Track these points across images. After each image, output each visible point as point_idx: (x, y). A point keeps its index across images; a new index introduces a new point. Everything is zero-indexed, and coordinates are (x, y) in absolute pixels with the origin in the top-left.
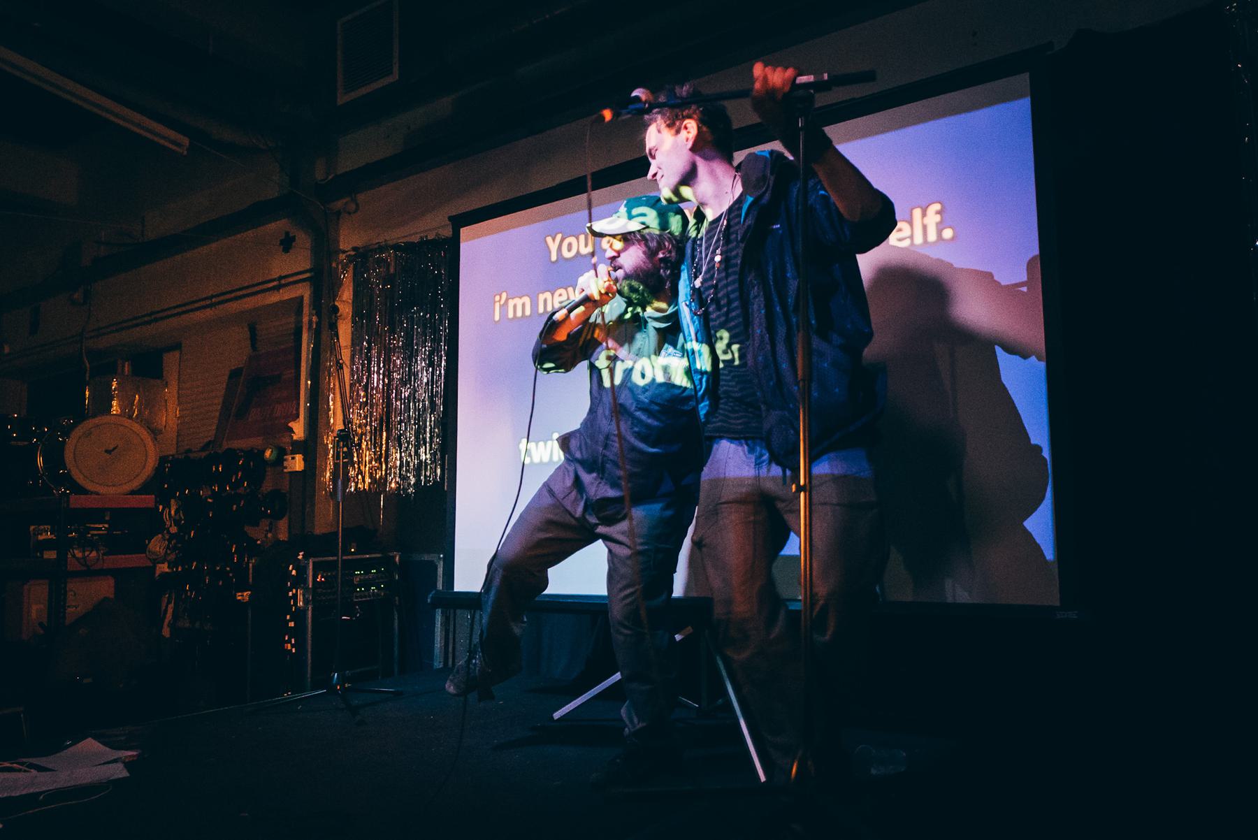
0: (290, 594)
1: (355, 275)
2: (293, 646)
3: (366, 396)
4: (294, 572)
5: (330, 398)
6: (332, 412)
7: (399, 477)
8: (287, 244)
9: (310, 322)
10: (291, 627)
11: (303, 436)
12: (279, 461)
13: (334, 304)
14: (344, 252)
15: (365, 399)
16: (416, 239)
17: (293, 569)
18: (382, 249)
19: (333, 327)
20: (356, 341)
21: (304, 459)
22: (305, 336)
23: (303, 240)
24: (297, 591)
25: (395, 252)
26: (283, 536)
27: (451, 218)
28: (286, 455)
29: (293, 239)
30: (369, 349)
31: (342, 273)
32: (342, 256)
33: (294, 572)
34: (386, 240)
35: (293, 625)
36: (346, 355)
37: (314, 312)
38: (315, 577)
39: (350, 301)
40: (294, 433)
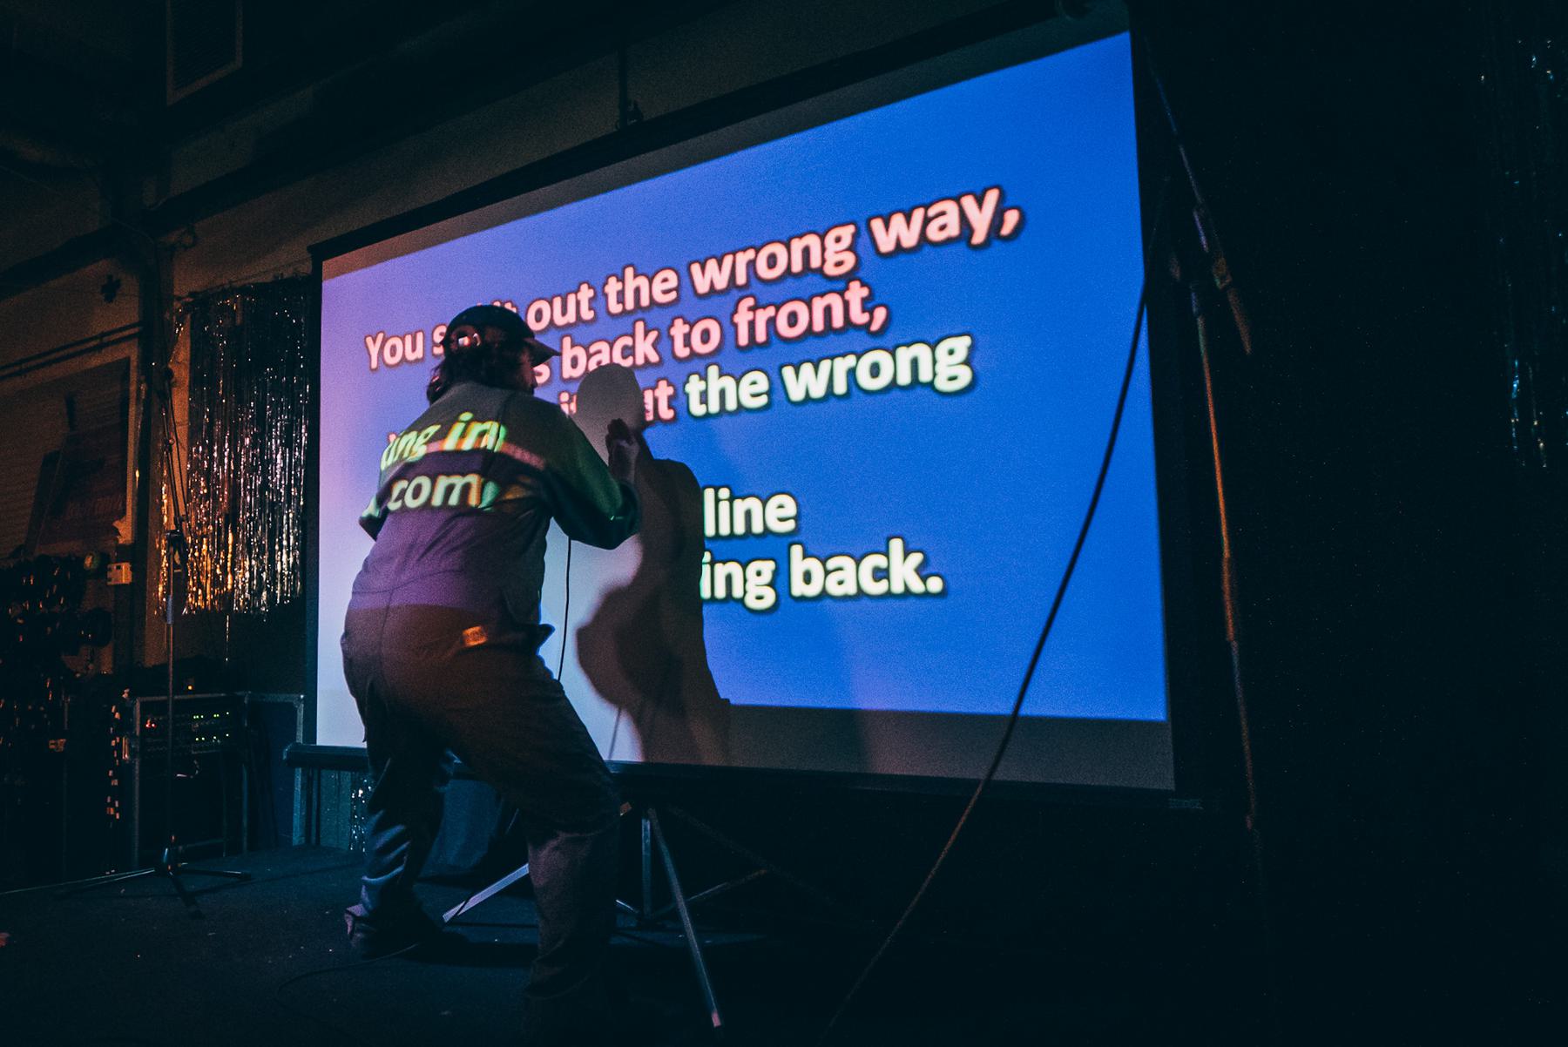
0: (113, 743)
1: (192, 328)
2: (117, 810)
3: (207, 487)
4: (117, 715)
5: (163, 489)
6: (165, 507)
7: (249, 593)
8: (111, 290)
9: (139, 390)
10: (114, 786)
11: (130, 539)
12: (102, 571)
13: (167, 368)
14: (179, 299)
15: (205, 491)
16: (269, 278)
17: (116, 711)
18: (226, 293)
19: (165, 398)
20: (194, 415)
21: (132, 569)
22: (132, 410)
23: (130, 285)
24: (121, 740)
25: (242, 297)
26: (106, 670)
27: (311, 249)
28: (109, 563)
29: (118, 284)
30: (211, 425)
31: (178, 326)
32: (177, 305)
33: (117, 715)
34: (231, 282)
35: (116, 784)
36: (182, 432)
37: (143, 378)
38: (143, 723)
39: (187, 363)
40: (119, 534)
